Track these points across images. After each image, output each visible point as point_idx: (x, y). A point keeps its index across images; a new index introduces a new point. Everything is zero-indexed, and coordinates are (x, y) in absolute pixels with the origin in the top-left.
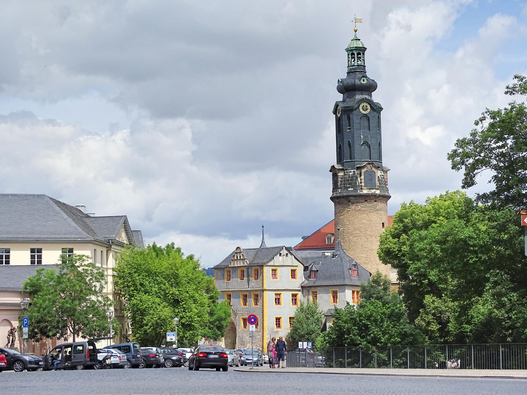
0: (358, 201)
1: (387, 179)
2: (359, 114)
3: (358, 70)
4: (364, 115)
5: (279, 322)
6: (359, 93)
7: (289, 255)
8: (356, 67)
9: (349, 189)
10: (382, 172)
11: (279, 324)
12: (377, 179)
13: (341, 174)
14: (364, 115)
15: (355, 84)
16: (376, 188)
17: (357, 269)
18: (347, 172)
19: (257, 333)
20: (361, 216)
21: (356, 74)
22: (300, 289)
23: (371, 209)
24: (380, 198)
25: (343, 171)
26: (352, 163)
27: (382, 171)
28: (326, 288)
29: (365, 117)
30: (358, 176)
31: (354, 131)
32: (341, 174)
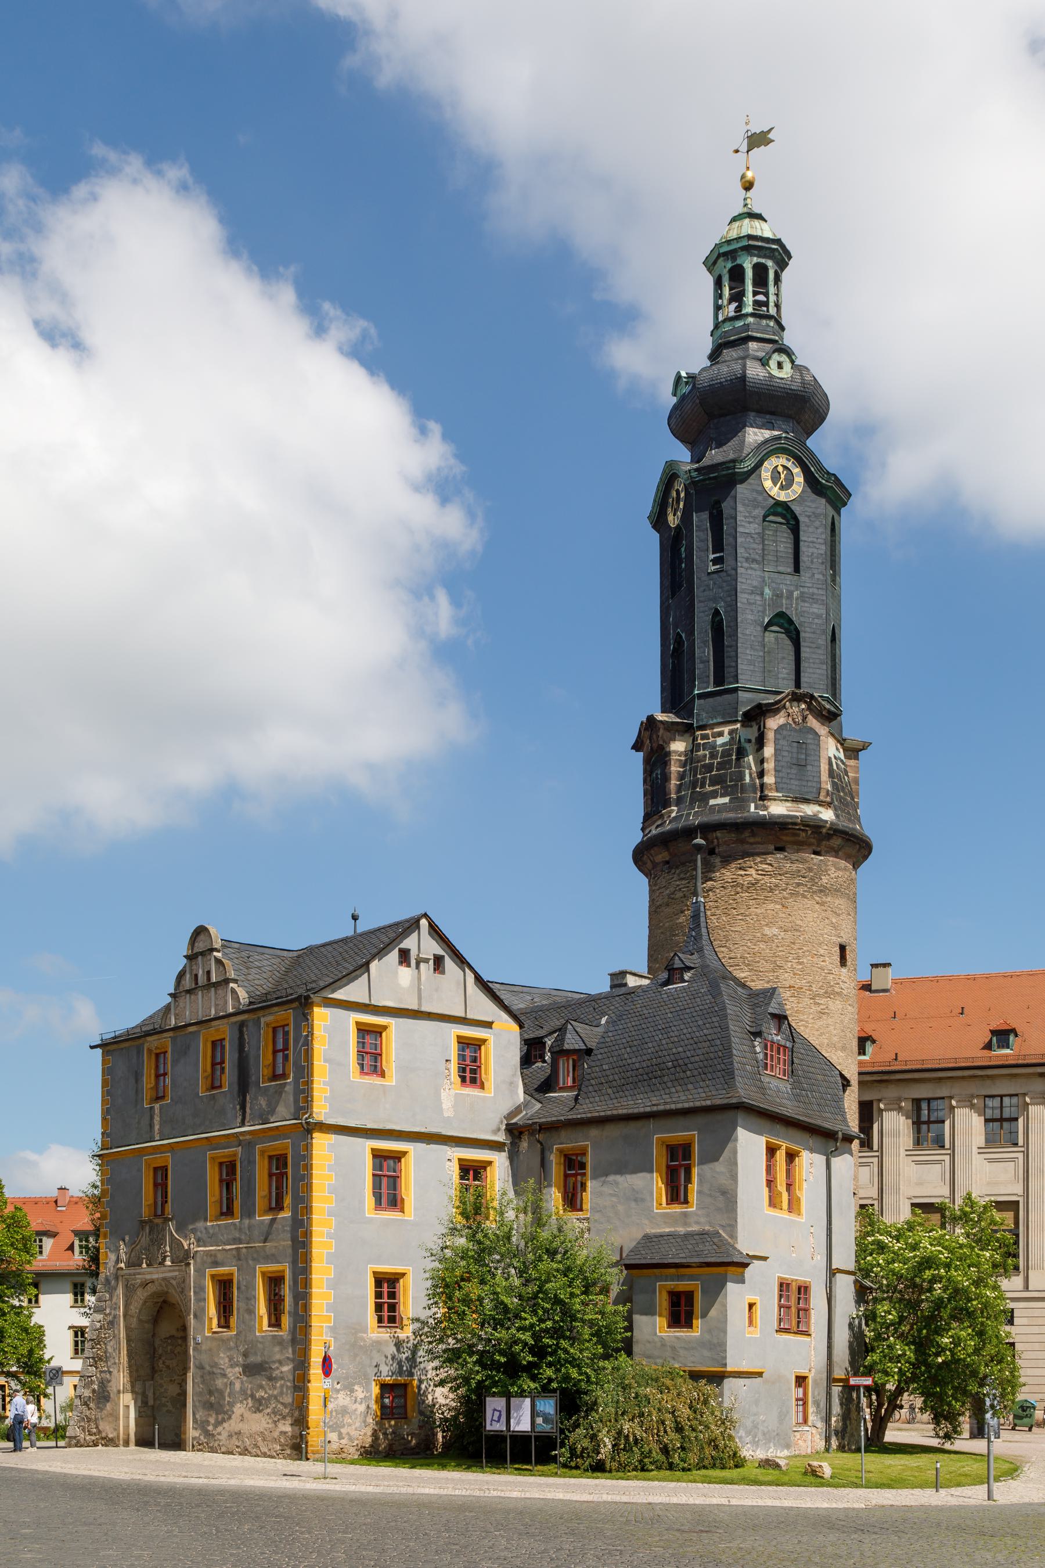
0: (747, 846)
1: (856, 781)
2: (760, 498)
3: (755, 334)
4: (780, 510)
5: (392, 1295)
6: (759, 421)
7: (449, 963)
8: (751, 320)
9: (712, 802)
10: (841, 750)
11: (393, 1308)
12: (824, 767)
13: (678, 746)
14: (780, 510)
15: (743, 378)
16: (822, 798)
17: (789, 1044)
18: (705, 737)
19: (277, 1349)
20: (758, 911)
21: (747, 349)
22: (501, 1137)
23: (798, 885)
24: (837, 842)
25: (687, 735)
26: (727, 697)
27: (842, 744)
28: (632, 1128)
29: (783, 516)
30: (751, 748)
31: (736, 570)
32: (678, 746)
